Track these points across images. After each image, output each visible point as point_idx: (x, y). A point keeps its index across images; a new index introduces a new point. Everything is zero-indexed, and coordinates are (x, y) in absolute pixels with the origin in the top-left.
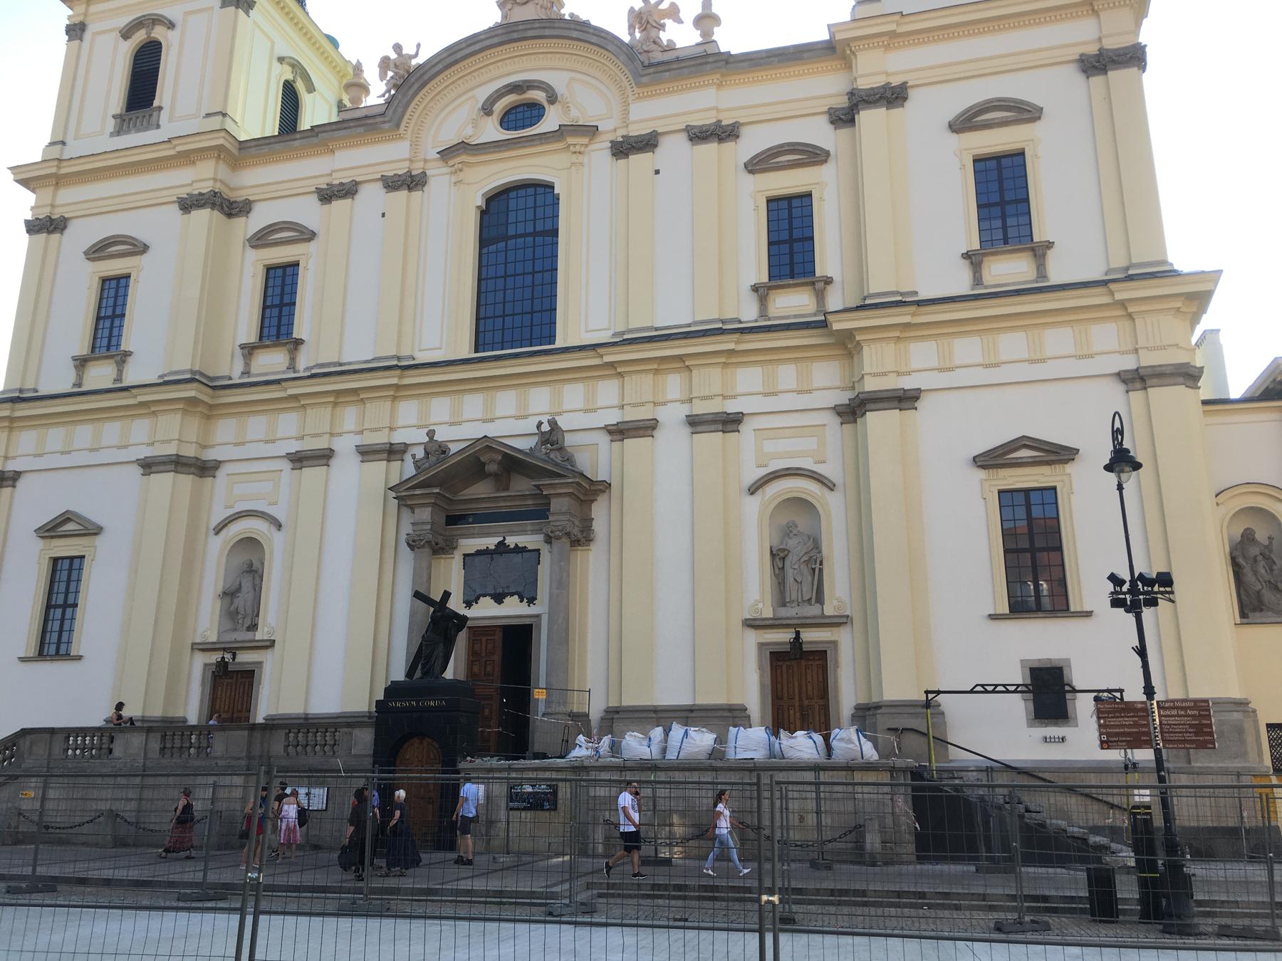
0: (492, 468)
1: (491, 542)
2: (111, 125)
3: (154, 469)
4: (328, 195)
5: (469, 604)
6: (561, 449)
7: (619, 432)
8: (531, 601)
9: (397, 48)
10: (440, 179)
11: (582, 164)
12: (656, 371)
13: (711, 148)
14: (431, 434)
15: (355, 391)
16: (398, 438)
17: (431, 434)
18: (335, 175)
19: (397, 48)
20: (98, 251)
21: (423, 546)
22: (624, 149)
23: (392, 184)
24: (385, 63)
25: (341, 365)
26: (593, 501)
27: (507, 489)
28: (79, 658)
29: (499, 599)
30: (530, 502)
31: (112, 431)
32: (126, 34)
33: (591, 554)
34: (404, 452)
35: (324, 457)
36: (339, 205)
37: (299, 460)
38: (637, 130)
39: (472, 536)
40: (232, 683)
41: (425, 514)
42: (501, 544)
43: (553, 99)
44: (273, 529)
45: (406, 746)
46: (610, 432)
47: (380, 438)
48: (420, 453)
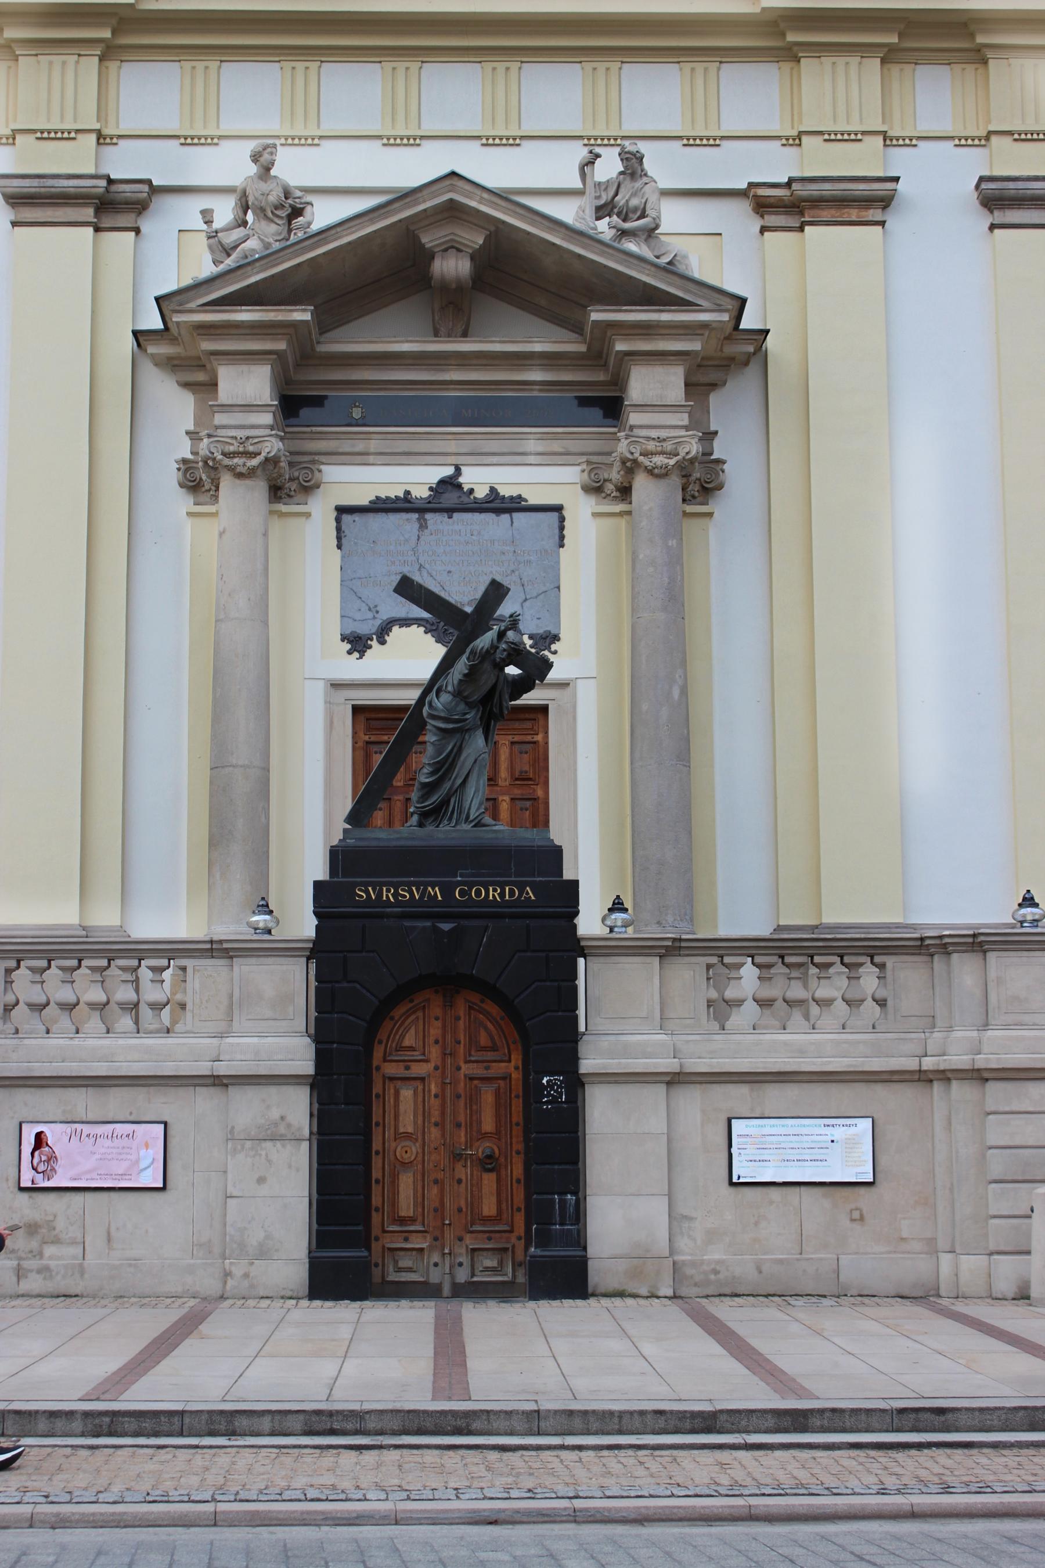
0: (453, 267)
1: (419, 479)
5: (358, 644)
6: (650, 233)
7: (787, 207)
12: (889, 56)
21: (251, 473)
26: (713, 386)
27: (465, 334)
30: (536, 375)
33: (714, 530)
34: (140, 207)
39: (361, 458)
41: (249, 385)
42: (451, 484)
45: (398, 1012)
46: (762, 206)
47: (76, 160)
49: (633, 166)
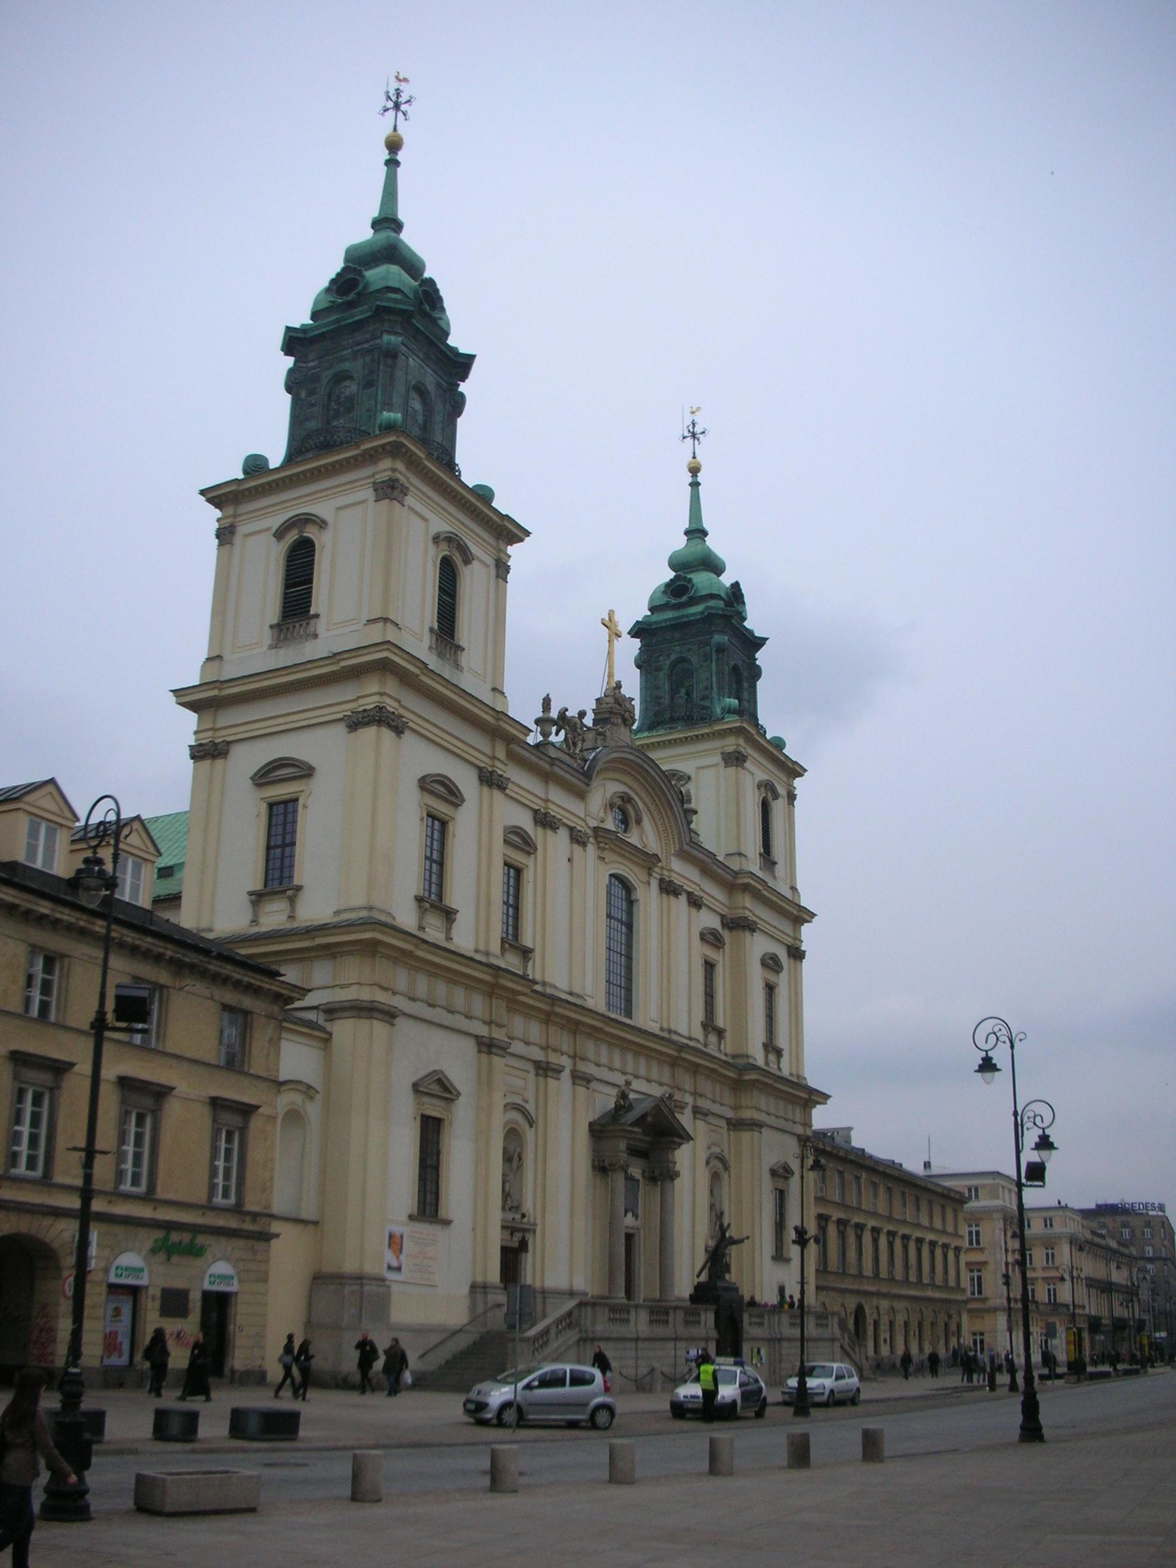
2: (427, 638)
3: (494, 1050)
4: (545, 821)
8: (636, 1216)
9: (582, 714)
10: (591, 849)
11: (649, 884)
13: (694, 911)
14: (628, 1083)
15: (578, 1023)
16: (590, 1069)
17: (628, 1083)
18: (550, 805)
19: (582, 714)
20: (428, 784)
22: (669, 888)
23: (577, 838)
24: (563, 713)
25: (556, 987)
28: (447, 1223)
29: (626, 1212)
31: (459, 997)
32: (436, 539)
35: (559, 1071)
36: (549, 832)
37: (544, 1070)
38: (678, 881)
40: (511, 1259)
43: (639, 822)
44: (527, 1126)
48: (614, 1092)
49: (671, 1097)
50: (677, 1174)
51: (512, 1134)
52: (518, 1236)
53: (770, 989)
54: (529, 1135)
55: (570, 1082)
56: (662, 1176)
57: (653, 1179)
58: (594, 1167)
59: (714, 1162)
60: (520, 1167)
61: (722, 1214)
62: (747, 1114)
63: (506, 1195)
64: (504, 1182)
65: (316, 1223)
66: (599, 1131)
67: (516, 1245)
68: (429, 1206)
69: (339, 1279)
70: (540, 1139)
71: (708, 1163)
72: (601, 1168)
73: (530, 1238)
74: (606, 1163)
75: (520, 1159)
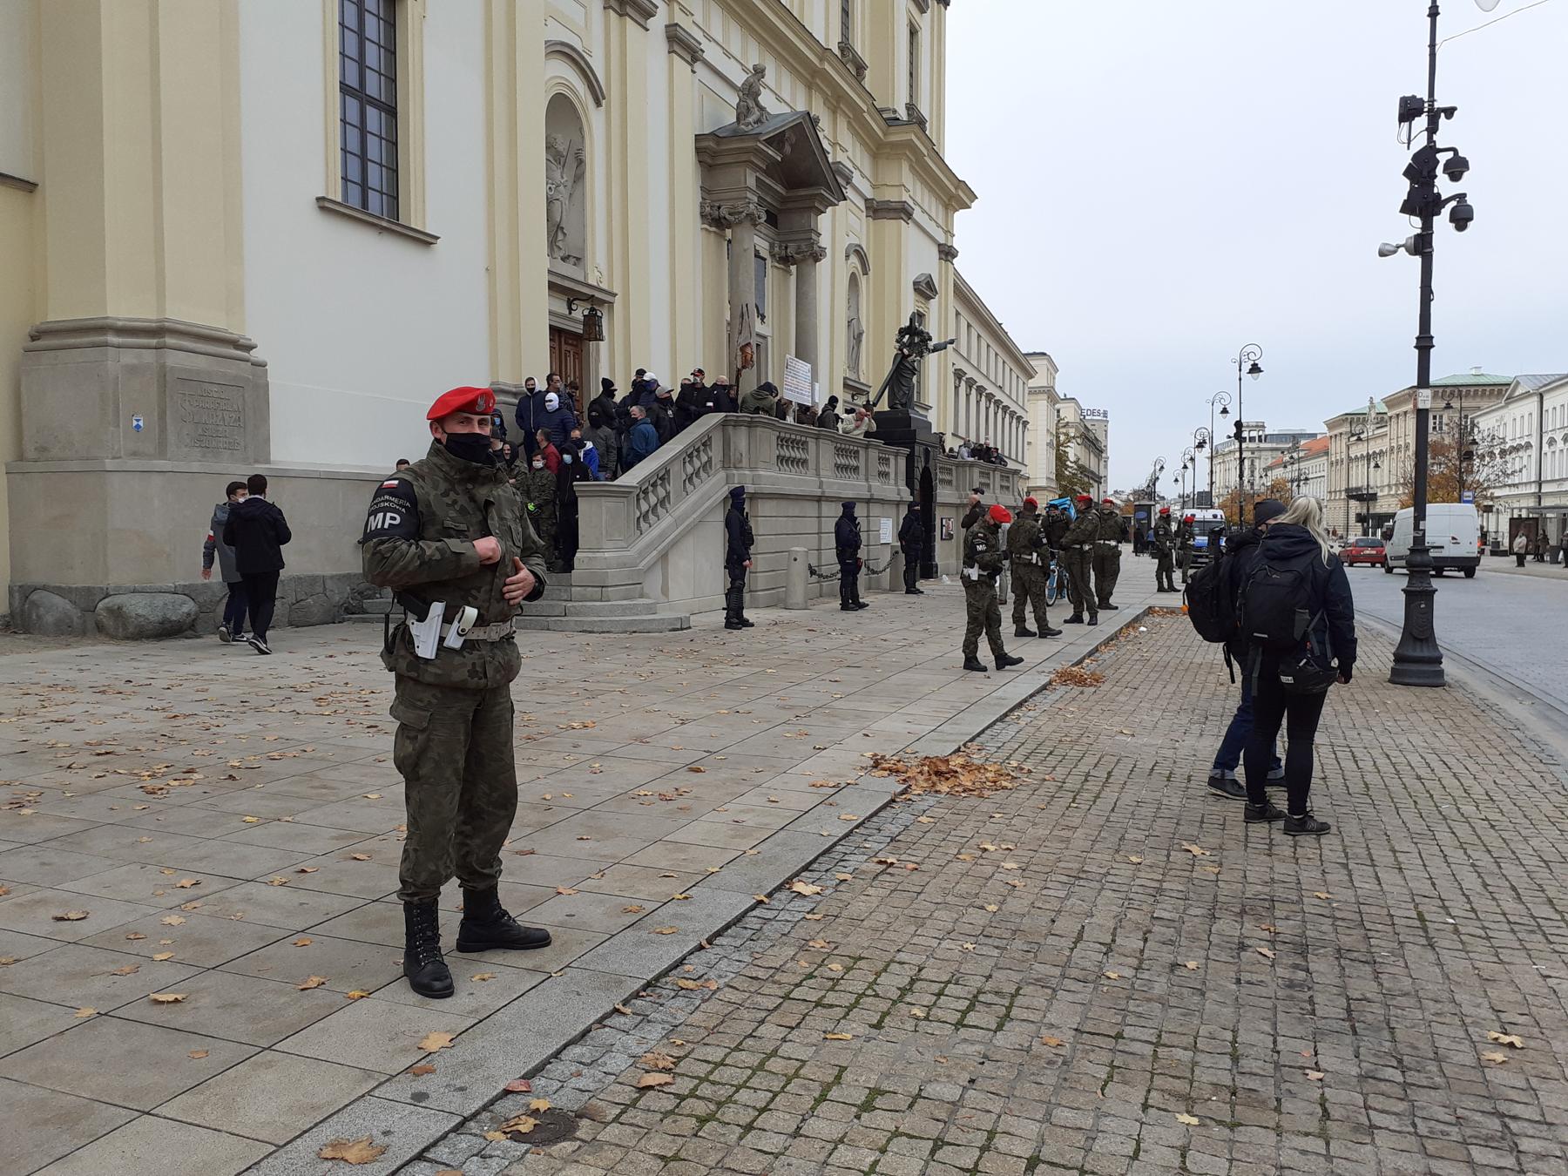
28: (425, 240)
50: (817, 256)
51: (561, 110)
52: (580, 312)
53: (913, 32)
54: (595, 120)
55: (662, 45)
56: (797, 253)
57: (786, 260)
58: (703, 216)
59: (854, 259)
60: (579, 178)
61: (860, 334)
62: (891, 195)
63: (555, 230)
64: (550, 202)
65: (29, 187)
66: (712, 153)
67: (579, 329)
68: (373, 190)
69: (94, 331)
70: (615, 130)
71: (847, 257)
72: (716, 220)
73: (603, 312)
74: (724, 212)
75: (580, 162)
